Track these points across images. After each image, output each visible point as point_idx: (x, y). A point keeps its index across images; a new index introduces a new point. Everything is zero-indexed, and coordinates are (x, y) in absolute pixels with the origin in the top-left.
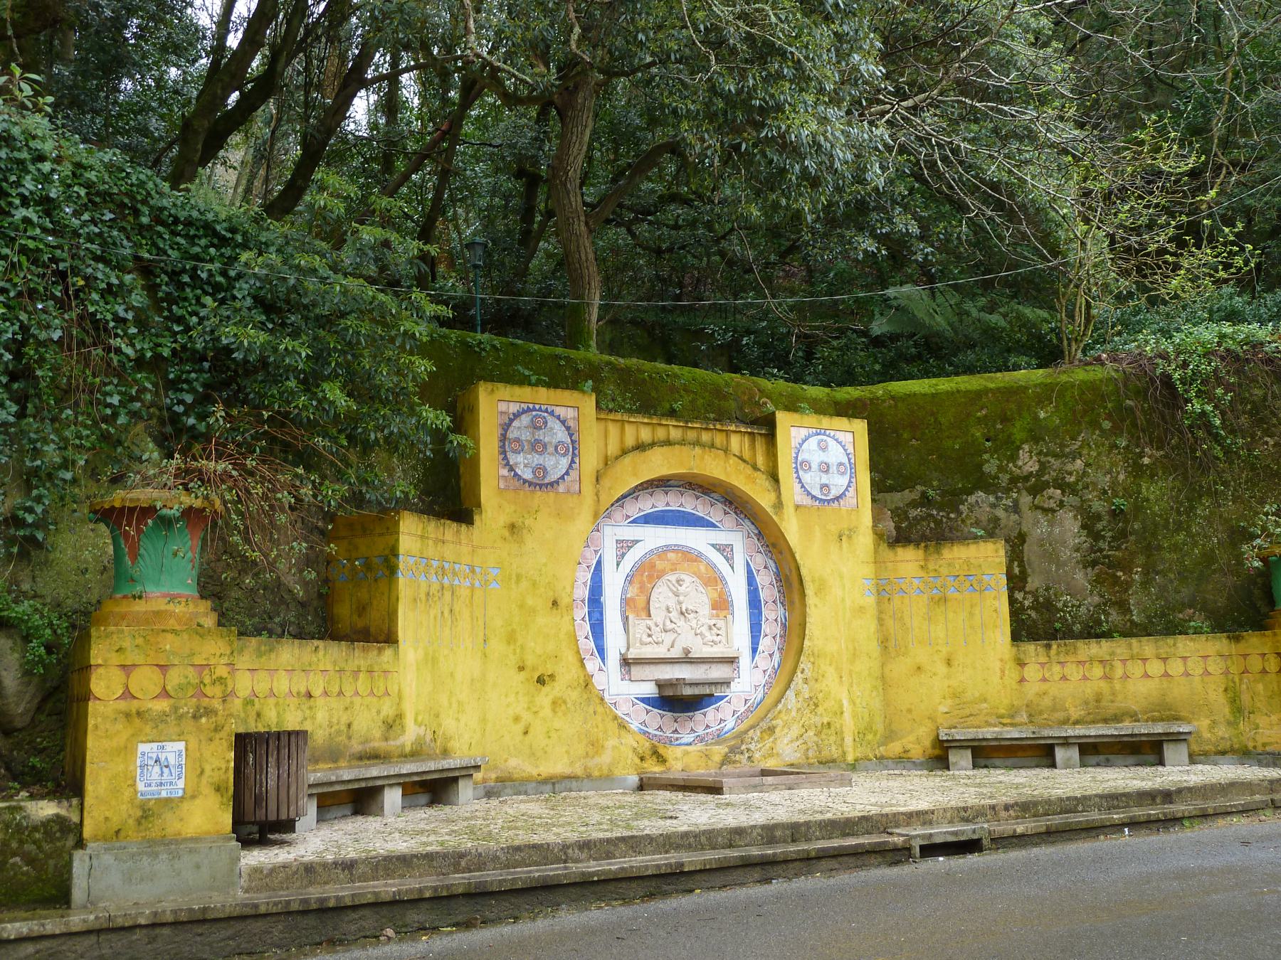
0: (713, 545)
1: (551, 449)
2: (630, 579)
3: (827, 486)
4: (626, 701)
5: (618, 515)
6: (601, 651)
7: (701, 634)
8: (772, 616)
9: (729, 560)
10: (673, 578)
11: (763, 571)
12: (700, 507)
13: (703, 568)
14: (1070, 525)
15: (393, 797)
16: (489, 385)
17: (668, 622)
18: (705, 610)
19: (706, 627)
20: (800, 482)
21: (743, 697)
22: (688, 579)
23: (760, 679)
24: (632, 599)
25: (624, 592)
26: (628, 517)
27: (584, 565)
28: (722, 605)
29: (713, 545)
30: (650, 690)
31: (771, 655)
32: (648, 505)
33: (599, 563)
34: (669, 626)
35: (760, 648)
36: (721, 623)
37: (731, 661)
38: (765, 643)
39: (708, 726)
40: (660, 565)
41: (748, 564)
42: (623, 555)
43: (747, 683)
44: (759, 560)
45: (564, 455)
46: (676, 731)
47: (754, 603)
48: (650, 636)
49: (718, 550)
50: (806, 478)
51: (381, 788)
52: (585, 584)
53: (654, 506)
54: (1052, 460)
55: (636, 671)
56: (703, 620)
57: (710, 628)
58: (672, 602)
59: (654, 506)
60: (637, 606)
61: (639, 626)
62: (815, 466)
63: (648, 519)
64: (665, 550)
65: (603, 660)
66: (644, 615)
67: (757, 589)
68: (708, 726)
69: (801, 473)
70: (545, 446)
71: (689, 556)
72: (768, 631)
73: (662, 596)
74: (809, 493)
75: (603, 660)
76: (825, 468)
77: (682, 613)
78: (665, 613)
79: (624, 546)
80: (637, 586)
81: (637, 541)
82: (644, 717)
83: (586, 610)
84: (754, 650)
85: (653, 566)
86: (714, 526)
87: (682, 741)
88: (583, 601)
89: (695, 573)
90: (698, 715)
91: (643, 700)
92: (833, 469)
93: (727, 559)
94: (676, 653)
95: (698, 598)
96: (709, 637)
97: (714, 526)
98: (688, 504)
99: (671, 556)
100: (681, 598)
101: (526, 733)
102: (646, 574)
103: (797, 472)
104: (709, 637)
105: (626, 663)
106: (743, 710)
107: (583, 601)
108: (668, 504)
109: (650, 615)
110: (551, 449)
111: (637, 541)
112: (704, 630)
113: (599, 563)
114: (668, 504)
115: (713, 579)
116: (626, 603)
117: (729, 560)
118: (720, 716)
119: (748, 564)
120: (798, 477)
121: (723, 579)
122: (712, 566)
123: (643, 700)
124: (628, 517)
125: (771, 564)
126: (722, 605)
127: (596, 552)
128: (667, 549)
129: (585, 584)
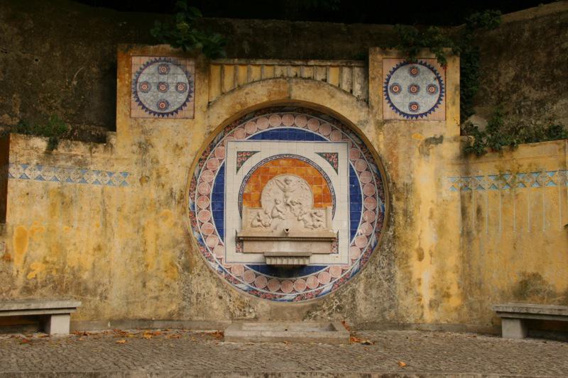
0: (320, 154)
1: (172, 88)
2: (247, 180)
3: (416, 104)
5: (239, 132)
6: (221, 231)
7: (303, 220)
8: (371, 208)
9: (335, 165)
10: (281, 178)
11: (364, 173)
13: (310, 171)
17: (275, 211)
18: (308, 202)
19: (308, 214)
20: (390, 101)
21: (341, 267)
23: (356, 254)
24: (249, 195)
25: (242, 189)
26: (248, 135)
27: (210, 170)
28: (325, 198)
29: (320, 154)
30: (255, 259)
31: (368, 237)
32: (264, 125)
33: (223, 169)
35: (359, 231)
36: (321, 212)
37: (332, 241)
39: (308, 289)
40: (271, 168)
41: (351, 168)
42: (242, 163)
43: (345, 256)
44: (360, 165)
46: (280, 291)
47: (355, 197)
48: (259, 221)
49: (325, 157)
50: (396, 99)
51: (49, 316)
52: (210, 183)
53: (270, 126)
55: (247, 246)
56: (305, 210)
57: (312, 216)
58: (280, 196)
59: (270, 126)
60: (249, 198)
61: (250, 214)
63: (265, 136)
65: (222, 237)
66: (257, 206)
67: (357, 187)
68: (308, 289)
69: (391, 95)
70: (168, 87)
71: (298, 163)
72: (366, 218)
73: (272, 191)
74: (397, 110)
75: (222, 237)
77: (288, 205)
79: (243, 157)
80: (252, 184)
81: (255, 152)
82: (253, 279)
84: (353, 233)
85: (267, 170)
86: (322, 139)
87: (287, 298)
88: (208, 196)
89: (302, 176)
90: (300, 280)
91: (253, 267)
93: (332, 164)
98: (300, 124)
99: (283, 162)
100: (287, 194)
102: (262, 175)
103: (387, 95)
105: (240, 241)
106: (339, 277)
107: (208, 196)
108: (282, 124)
109: (261, 206)
110: (172, 88)
111: (255, 152)
112: (306, 217)
113: (223, 169)
114: (282, 124)
115: (319, 180)
116: (243, 197)
117: (335, 165)
118: (319, 281)
121: (328, 180)
122: (319, 170)
124: (248, 135)
125: (372, 167)
126: (325, 198)
127: (221, 161)
128: (281, 157)
129: (210, 183)
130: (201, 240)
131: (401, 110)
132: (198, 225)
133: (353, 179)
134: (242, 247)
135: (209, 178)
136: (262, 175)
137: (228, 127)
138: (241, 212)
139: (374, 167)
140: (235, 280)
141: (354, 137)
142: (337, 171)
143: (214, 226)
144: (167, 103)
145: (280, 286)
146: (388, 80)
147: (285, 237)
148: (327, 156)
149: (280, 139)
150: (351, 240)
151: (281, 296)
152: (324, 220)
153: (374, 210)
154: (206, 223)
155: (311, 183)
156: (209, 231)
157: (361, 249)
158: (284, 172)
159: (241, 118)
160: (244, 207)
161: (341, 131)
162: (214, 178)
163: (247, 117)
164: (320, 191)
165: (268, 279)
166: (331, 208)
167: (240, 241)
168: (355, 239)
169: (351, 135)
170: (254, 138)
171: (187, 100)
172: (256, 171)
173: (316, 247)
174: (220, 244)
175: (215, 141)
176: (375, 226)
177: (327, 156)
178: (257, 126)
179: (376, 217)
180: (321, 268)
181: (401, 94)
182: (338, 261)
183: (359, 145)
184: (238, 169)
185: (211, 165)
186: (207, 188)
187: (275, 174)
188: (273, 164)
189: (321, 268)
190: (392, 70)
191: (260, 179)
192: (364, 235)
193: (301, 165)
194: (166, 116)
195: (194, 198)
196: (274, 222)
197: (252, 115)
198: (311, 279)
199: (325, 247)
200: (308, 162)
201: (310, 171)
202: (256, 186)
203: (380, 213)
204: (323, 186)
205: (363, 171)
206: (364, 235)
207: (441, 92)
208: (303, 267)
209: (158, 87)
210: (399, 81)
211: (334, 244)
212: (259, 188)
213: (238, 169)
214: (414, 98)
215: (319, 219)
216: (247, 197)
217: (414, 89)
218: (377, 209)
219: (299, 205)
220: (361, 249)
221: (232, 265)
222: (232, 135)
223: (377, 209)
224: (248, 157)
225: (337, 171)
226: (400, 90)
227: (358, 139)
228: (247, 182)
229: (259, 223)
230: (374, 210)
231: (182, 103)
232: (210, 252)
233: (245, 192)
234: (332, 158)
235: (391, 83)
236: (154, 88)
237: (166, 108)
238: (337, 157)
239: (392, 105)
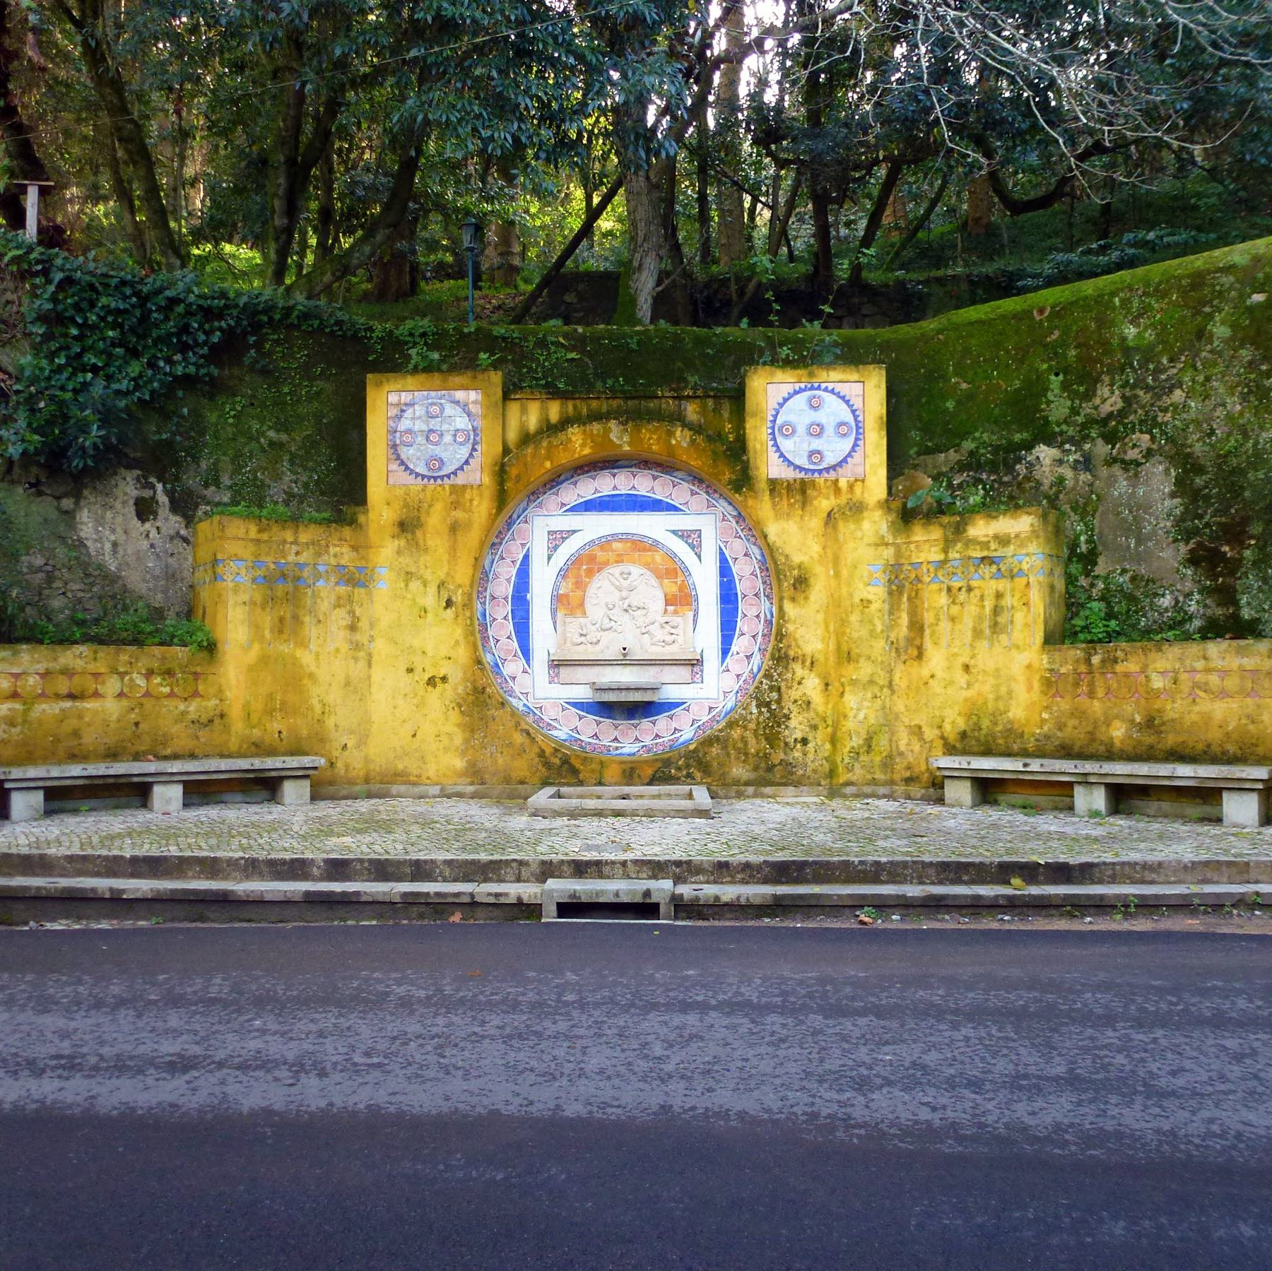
0: (674, 532)
1: (448, 438)
2: (563, 574)
3: (819, 452)
4: (554, 705)
5: (551, 500)
6: (526, 652)
8: (752, 612)
9: (696, 548)
10: (616, 570)
12: (658, 489)
13: (658, 558)
14: (1159, 482)
15: (168, 796)
16: (378, 376)
20: (778, 450)
21: (707, 704)
22: (636, 570)
23: (730, 683)
24: (566, 596)
25: (556, 587)
27: (508, 560)
29: (674, 532)
30: (583, 693)
32: (588, 488)
33: (526, 557)
34: (607, 624)
35: (734, 649)
37: (695, 664)
38: (739, 645)
41: (722, 553)
42: (556, 548)
44: (736, 547)
45: (461, 444)
47: (728, 597)
49: (681, 537)
50: (786, 445)
52: (508, 580)
54: (1141, 393)
62: (801, 430)
63: (588, 506)
64: (605, 542)
65: (528, 661)
69: (780, 439)
71: (640, 546)
72: (745, 629)
74: (790, 463)
75: (528, 661)
76: (817, 430)
78: (604, 610)
79: (558, 538)
80: (571, 581)
81: (574, 532)
82: (576, 722)
83: (509, 608)
84: (725, 652)
85: (592, 559)
86: (676, 509)
88: (506, 599)
89: (647, 566)
90: (645, 723)
91: (575, 705)
92: (830, 430)
93: (692, 547)
94: (613, 653)
95: (650, 593)
96: (660, 634)
97: (676, 509)
99: (616, 545)
101: (414, 736)
102: (585, 566)
103: (774, 439)
104: (660, 634)
105: (556, 665)
106: (705, 719)
108: (615, 488)
110: (448, 438)
111: (574, 532)
113: (526, 557)
115: (672, 570)
116: (558, 600)
117: (696, 548)
118: (674, 725)
119: (722, 553)
120: (776, 445)
121: (686, 571)
122: (672, 556)
123: (575, 705)
126: (682, 599)
127: (523, 545)
128: (615, 537)
129: (508, 580)
130: (497, 665)
131: (797, 462)
132: (492, 643)
133: (725, 570)
134: (557, 675)
135: (506, 573)
136: (585, 566)
137: (533, 493)
138: (555, 623)
139: (757, 551)
140: (549, 724)
141: (726, 504)
142: (699, 557)
143: (516, 644)
144: (441, 461)
145: (616, 733)
146: (775, 416)
147: (625, 660)
148: (683, 535)
149: (613, 510)
150: (723, 662)
151: (617, 748)
152: (681, 633)
153: (758, 616)
154: (503, 640)
155: (659, 577)
156: (509, 651)
157: (738, 676)
158: (619, 561)
159: (553, 480)
160: (560, 615)
161: (705, 496)
162: (514, 572)
163: (562, 478)
164: (673, 589)
165: (598, 723)
166: (691, 614)
167: (556, 665)
168: (728, 659)
169: (721, 501)
170: (572, 509)
171: (471, 455)
172: (576, 561)
173: (669, 674)
174: (525, 672)
175: (515, 516)
176: (759, 638)
177: (683, 535)
178: (577, 491)
179: (761, 627)
180: (678, 705)
181: (795, 438)
182: (702, 694)
183: (734, 517)
184: (549, 558)
185: (509, 552)
186: (503, 586)
187: (606, 563)
188: (602, 548)
189: (678, 705)
190: (781, 401)
191: (583, 573)
192: (741, 655)
193: (645, 550)
194: (439, 481)
195: (484, 603)
196: (606, 638)
197: (568, 475)
198: (662, 723)
199: (684, 672)
200: (655, 545)
201: (658, 558)
202: (577, 582)
203: (766, 621)
204: (679, 581)
205: (740, 556)
206: (741, 655)
207: (858, 433)
208: (650, 704)
209: (427, 438)
210: (792, 418)
211: (696, 669)
212: (580, 585)
213: (549, 558)
214: (816, 444)
215: (673, 631)
216: (565, 602)
217: (817, 430)
218: (762, 615)
219: (644, 612)
220: (738, 676)
221: (544, 703)
222: (540, 506)
223: (762, 615)
224: (564, 539)
225: (699, 557)
226: (794, 432)
227: (730, 508)
228: (564, 577)
229: (583, 639)
230: (758, 616)
231: (463, 461)
232: (511, 684)
233: (561, 592)
234: (691, 538)
235: (779, 422)
236: (420, 439)
237: (440, 469)
238: (700, 536)
239: (782, 455)
